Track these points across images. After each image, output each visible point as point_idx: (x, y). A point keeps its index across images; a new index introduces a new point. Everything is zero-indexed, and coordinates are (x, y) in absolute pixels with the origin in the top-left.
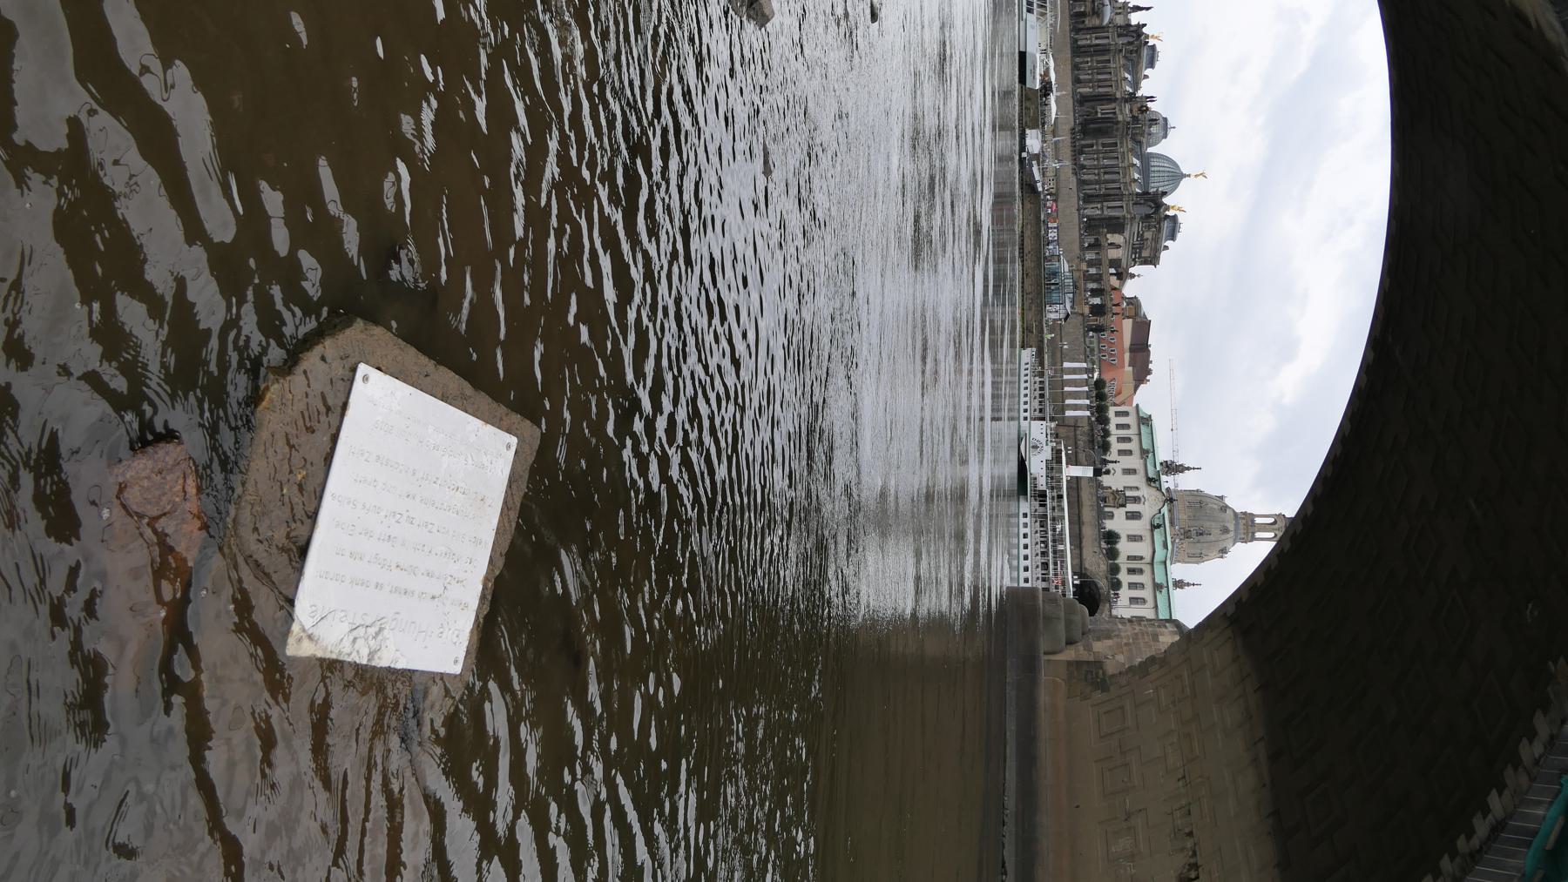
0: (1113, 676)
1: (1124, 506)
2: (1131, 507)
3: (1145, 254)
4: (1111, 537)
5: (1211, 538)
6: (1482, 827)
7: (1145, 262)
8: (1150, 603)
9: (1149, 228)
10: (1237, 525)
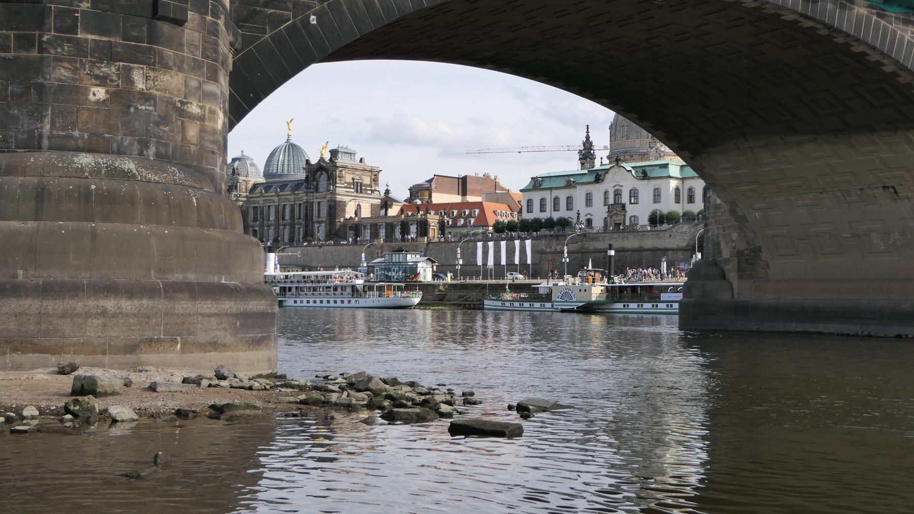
0: (748, 243)
1: (624, 206)
3: (367, 180)
4: (656, 219)
6: (808, 24)
7: (375, 180)
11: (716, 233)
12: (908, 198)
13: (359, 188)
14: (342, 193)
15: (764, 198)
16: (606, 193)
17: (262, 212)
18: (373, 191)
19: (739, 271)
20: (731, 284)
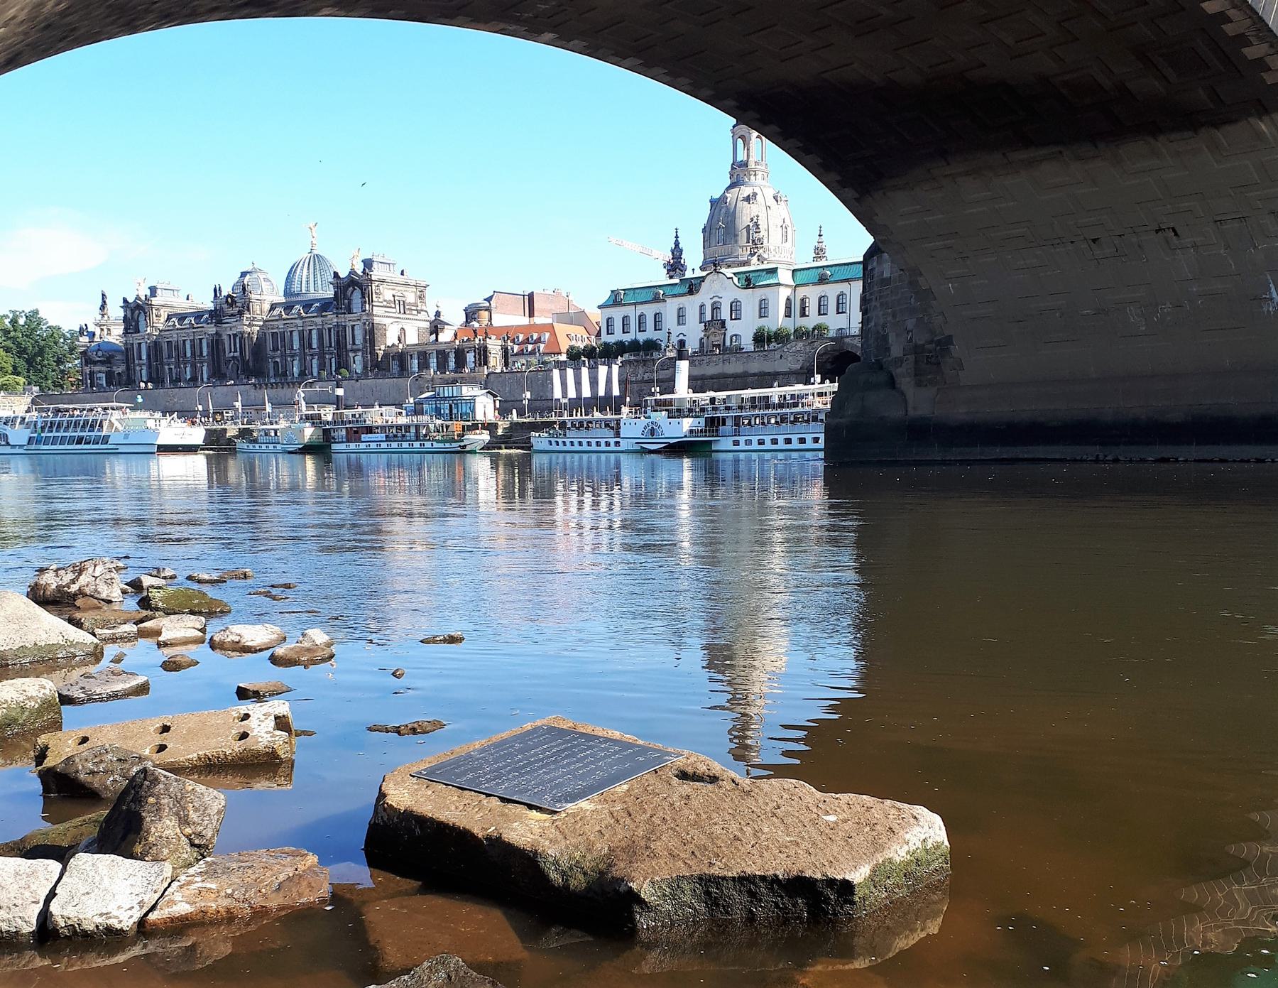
1: (723, 322)
3: (411, 297)
8: (843, 287)
11: (882, 321)
12: (1195, 246)
13: (403, 307)
14: (381, 315)
16: (702, 306)
17: (283, 339)
18: (419, 312)
20: (903, 394)
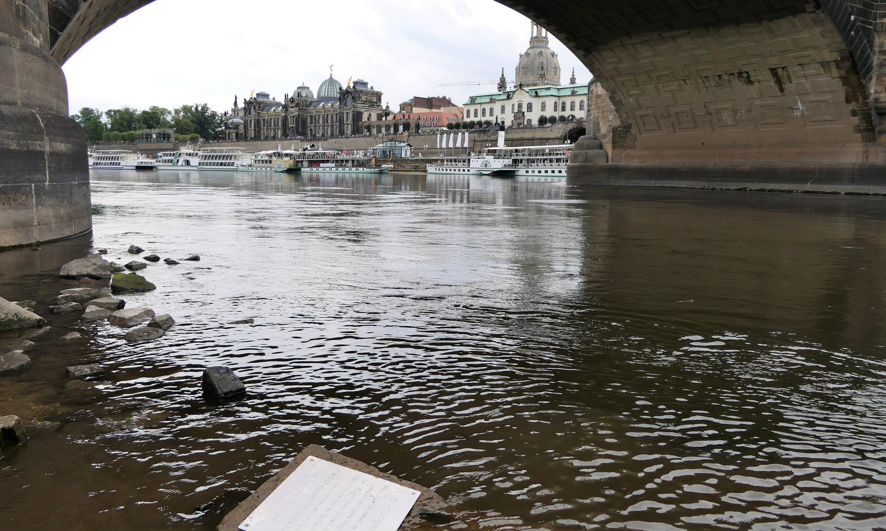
0: (622, 122)
2: (524, 109)
3: (375, 100)
4: (543, 121)
5: (545, 61)
7: (379, 99)
9: (359, 97)
10: (538, 47)
12: (759, 82)
15: (638, 86)
19: (613, 143)
